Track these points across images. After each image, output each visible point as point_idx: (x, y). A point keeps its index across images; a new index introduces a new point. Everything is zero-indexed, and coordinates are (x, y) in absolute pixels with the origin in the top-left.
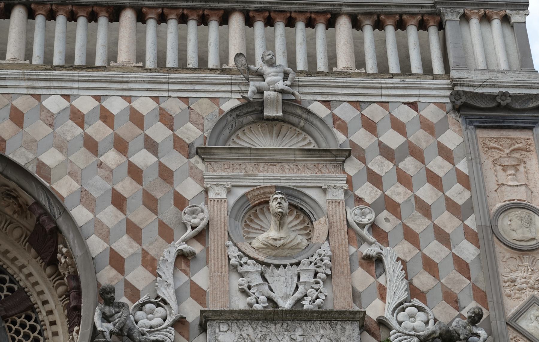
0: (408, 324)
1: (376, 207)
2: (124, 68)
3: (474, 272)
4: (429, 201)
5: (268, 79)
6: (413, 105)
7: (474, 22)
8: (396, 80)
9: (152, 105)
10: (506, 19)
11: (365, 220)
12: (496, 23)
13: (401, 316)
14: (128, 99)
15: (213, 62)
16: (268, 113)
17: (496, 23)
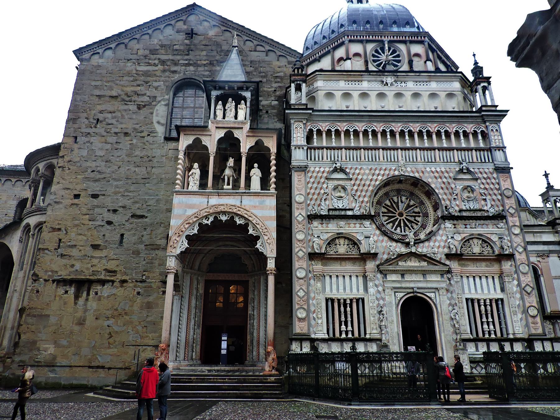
0: (492, 211)
1: (484, 189)
2: (438, 162)
3: (501, 201)
4: (492, 188)
5: (464, 164)
6: (488, 168)
7: (497, 151)
8: (485, 164)
9: (444, 169)
10: (502, 150)
11: (483, 192)
12: (501, 151)
13: (490, 209)
14: (440, 168)
15: (452, 160)
16: (464, 171)
17: (501, 151)
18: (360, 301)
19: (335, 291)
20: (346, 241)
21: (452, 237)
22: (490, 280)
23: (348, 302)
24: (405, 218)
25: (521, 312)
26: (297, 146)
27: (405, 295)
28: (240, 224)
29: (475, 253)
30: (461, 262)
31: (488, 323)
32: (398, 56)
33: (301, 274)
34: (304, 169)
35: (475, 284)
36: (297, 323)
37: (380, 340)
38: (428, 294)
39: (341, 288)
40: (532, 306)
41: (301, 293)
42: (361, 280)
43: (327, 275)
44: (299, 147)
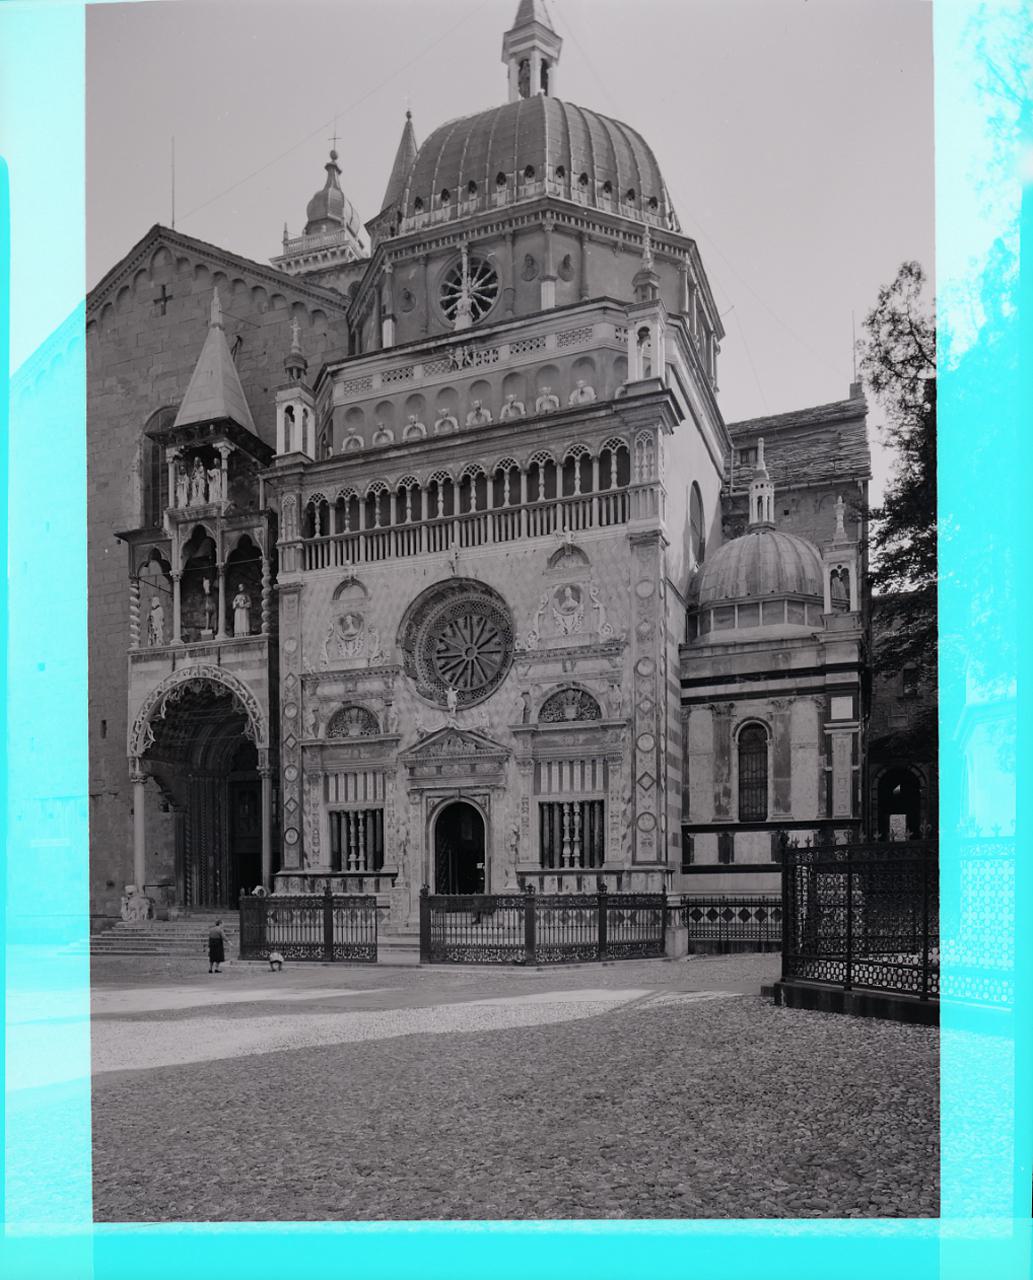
18: (376, 816)
19: (341, 798)
20: (361, 714)
21: (524, 693)
22: (588, 768)
23: (360, 816)
24: (479, 653)
25: (626, 824)
26: (286, 544)
27: (442, 801)
28: (220, 696)
29: (567, 720)
30: (538, 739)
31: (572, 844)
32: (492, 293)
33: (290, 774)
34: (296, 589)
35: (561, 776)
36: (285, 850)
37: (396, 875)
38: (476, 799)
39: (351, 795)
40: (648, 813)
41: (292, 806)
42: (379, 777)
43: (332, 774)
44: (290, 545)
